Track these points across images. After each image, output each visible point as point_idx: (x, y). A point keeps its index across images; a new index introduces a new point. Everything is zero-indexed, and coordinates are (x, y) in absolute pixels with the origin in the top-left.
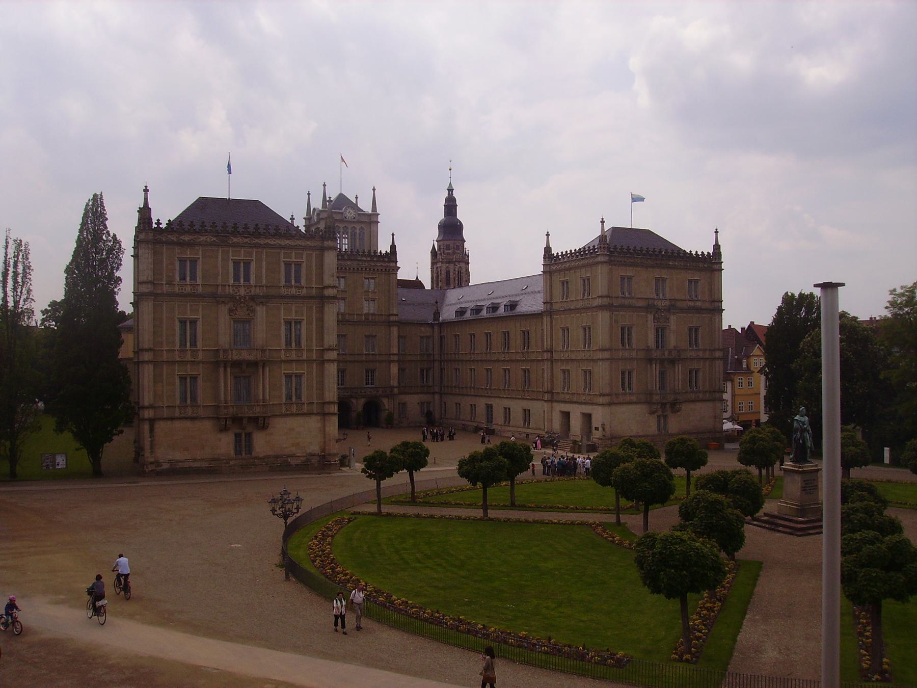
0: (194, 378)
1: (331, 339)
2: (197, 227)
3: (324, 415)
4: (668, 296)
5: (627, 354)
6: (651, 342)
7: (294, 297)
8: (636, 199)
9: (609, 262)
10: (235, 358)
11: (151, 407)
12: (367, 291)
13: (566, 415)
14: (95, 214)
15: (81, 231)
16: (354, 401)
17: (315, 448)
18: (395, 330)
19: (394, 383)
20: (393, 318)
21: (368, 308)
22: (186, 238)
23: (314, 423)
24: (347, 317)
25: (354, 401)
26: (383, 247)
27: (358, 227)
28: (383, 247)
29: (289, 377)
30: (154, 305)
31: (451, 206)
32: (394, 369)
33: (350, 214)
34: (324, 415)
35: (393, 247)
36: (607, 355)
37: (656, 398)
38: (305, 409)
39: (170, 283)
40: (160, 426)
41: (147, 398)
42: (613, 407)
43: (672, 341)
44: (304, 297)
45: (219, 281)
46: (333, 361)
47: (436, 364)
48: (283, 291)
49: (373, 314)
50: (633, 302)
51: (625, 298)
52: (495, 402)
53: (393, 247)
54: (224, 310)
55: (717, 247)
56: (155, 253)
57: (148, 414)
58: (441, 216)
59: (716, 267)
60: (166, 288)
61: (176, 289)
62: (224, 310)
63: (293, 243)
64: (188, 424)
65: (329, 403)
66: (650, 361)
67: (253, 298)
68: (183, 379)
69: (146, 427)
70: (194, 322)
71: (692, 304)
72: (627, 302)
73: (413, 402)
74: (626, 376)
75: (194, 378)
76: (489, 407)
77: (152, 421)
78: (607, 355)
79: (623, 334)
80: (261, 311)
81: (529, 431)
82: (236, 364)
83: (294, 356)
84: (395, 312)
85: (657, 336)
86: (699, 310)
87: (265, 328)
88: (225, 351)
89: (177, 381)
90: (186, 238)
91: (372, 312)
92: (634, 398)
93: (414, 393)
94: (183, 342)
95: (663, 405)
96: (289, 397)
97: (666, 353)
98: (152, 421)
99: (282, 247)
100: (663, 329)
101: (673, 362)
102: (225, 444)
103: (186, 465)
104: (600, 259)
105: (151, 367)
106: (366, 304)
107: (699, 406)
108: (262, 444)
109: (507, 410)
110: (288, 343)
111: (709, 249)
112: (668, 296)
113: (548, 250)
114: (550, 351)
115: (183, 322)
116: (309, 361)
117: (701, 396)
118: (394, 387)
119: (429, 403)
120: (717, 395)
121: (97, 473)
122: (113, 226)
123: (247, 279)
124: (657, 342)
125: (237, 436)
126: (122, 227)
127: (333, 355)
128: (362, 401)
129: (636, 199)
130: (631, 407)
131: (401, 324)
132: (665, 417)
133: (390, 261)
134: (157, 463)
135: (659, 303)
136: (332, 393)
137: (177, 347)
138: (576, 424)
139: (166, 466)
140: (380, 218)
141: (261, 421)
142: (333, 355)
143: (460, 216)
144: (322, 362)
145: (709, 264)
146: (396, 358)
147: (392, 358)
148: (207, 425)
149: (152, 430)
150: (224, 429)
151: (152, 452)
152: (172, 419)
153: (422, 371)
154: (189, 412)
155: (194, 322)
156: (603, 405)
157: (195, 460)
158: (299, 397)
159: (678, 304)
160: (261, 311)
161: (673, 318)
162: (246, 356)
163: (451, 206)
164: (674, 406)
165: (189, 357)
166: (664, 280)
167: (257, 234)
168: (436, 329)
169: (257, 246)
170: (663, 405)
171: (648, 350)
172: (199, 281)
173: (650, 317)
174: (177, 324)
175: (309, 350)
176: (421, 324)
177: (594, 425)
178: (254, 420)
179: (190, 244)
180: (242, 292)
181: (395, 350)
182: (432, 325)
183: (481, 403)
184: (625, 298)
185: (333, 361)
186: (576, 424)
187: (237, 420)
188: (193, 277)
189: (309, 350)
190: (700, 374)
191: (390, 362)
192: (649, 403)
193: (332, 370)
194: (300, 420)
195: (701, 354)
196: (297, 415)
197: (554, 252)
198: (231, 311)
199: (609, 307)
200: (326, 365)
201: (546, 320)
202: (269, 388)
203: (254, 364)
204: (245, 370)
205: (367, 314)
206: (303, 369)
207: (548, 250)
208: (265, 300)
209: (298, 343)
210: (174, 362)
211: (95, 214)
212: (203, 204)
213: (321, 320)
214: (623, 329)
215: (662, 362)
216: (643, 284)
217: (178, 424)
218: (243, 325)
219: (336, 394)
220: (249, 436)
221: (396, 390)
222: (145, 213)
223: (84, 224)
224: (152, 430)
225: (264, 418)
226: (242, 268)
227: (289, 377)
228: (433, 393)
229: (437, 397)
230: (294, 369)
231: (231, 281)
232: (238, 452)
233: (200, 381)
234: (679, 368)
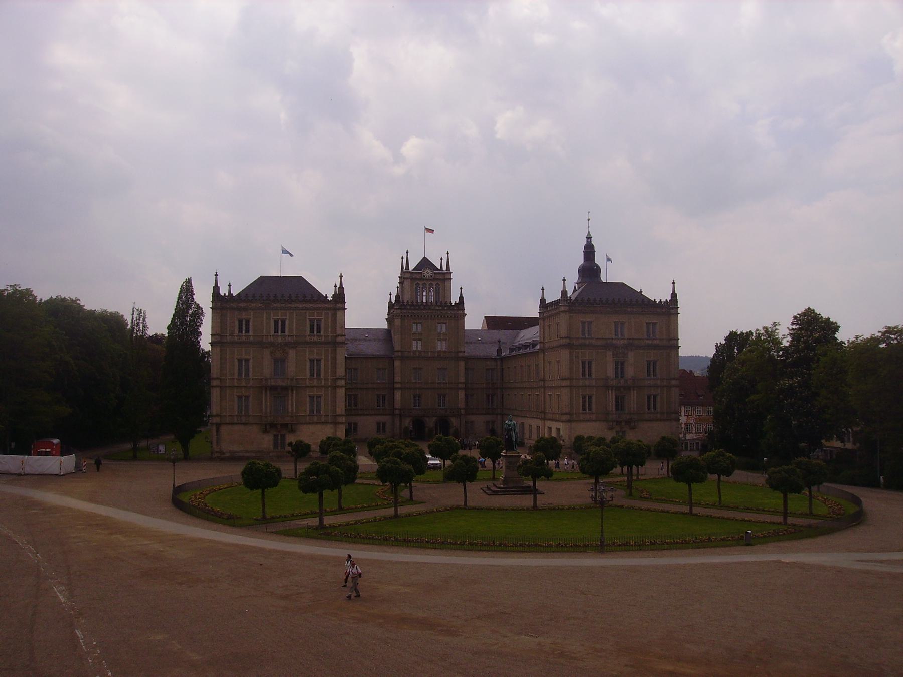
0: (247, 397)
1: (341, 371)
2: (251, 298)
3: (336, 423)
4: (626, 336)
5: (587, 382)
6: (610, 372)
7: (315, 343)
9: (570, 311)
10: (273, 384)
11: (217, 415)
12: (440, 334)
13: (550, 428)
14: (187, 291)
15: (178, 303)
16: (427, 419)
18: (462, 364)
19: (462, 405)
20: (461, 354)
21: (441, 346)
22: (243, 305)
24: (423, 354)
25: (427, 419)
26: (454, 300)
27: (434, 283)
28: (454, 300)
29: (311, 397)
30: (221, 350)
32: (462, 394)
33: (428, 273)
34: (336, 423)
35: (461, 298)
36: (567, 383)
39: (232, 335)
40: (224, 429)
41: (215, 409)
42: (574, 424)
43: (630, 372)
44: (321, 343)
45: (265, 333)
46: (342, 386)
48: (308, 339)
49: (445, 352)
50: (594, 341)
51: (585, 339)
53: (461, 298)
54: (267, 352)
55: (674, 295)
57: (216, 420)
58: (581, 261)
59: (672, 311)
60: (229, 339)
62: (267, 352)
63: (315, 306)
64: (242, 427)
65: (339, 415)
68: (240, 397)
69: (214, 428)
70: (247, 361)
71: (650, 342)
72: (587, 342)
73: (479, 421)
75: (247, 397)
77: (218, 426)
78: (567, 383)
79: (584, 367)
80: (292, 353)
82: (273, 388)
83: (315, 383)
84: (462, 349)
85: (616, 368)
86: (656, 347)
87: (296, 365)
88: (266, 379)
89: (236, 399)
90: (243, 305)
92: (594, 417)
94: (240, 374)
96: (312, 411)
97: (622, 381)
98: (218, 426)
99: (307, 309)
100: (622, 364)
103: (241, 454)
104: (563, 309)
105: (218, 389)
106: (439, 343)
110: (312, 374)
111: (666, 297)
112: (626, 336)
114: (544, 380)
115: (240, 361)
116: (326, 387)
117: (659, 416)
119: (493, 422)
120: (674, 416)
121: (186, 458)
122: (197, 298)
123: (283, 331)
124: (616, 373)
125: (276, 436)
126: (203, 298)
127: (343, 382)
128: (435, 418)
131: (467, 359)
133: (458, 310)
134: (222, 453)
135: (614, 342)
137: (236, 377)
139: (228, 455)
140: (452, 276)
141: (290, 426)
142: (343, 382)
144: (335, 387)
145: (670, 308)
146: (463, 386)
147: (460, 385)
149: (218, 431)
150: (266, 431)
151: (217, 445)
152: (232, 424)
153: (488, 396)
154: (244, 420)
155: (247, 361)
156: (563, 421)
157: (247, 452)
158: (318, 411)
160: (292, 353)
162: (280, 383)
165: (244, 384)
166: (622, 324)
167: (290, 301)
168: (499, 362)
169: (290, 309)
170: (618, 423)
172: (251, 333)
173: (609, 353)
174: (236, 361)
176: (486, 358)
178: (285, 426)
179: (245, 309)
180: (280, 340)
181: (462, 380)
182: (495, 359)
184: (585, 339)
185: (342, 386)
187: (273, 425)
188: (247, 331)
190: (658, 399)
193: (341, 393)
194: (319, 427)
195: (659, 382)
196: (317, 423)
198: (272, 353)
199: (570, 346)
200: (337, 390)
201: (541, 355)
203: (286, 388)
204: (280, 392)
205: (439, 352)
206: (321, 393)
207: (543, 301)
208: (295, 345)
209: (319, 374)
211: (187, 291)
212: (263, 281)
213: (334, 359)
214: (584, 363)
216: (604, 326)
217: (236, 428)
218: (280, 363)
219: (344, 409)
221: (463, 412)
222: (216, 288)
223: (180, 298)
224: (218, 431)
225: (292, 425)
226: (280, 326)
227: (311, 397)
229: (499, 417)
230: (315, 392)
231: (273, 333)
233: (251, 399)
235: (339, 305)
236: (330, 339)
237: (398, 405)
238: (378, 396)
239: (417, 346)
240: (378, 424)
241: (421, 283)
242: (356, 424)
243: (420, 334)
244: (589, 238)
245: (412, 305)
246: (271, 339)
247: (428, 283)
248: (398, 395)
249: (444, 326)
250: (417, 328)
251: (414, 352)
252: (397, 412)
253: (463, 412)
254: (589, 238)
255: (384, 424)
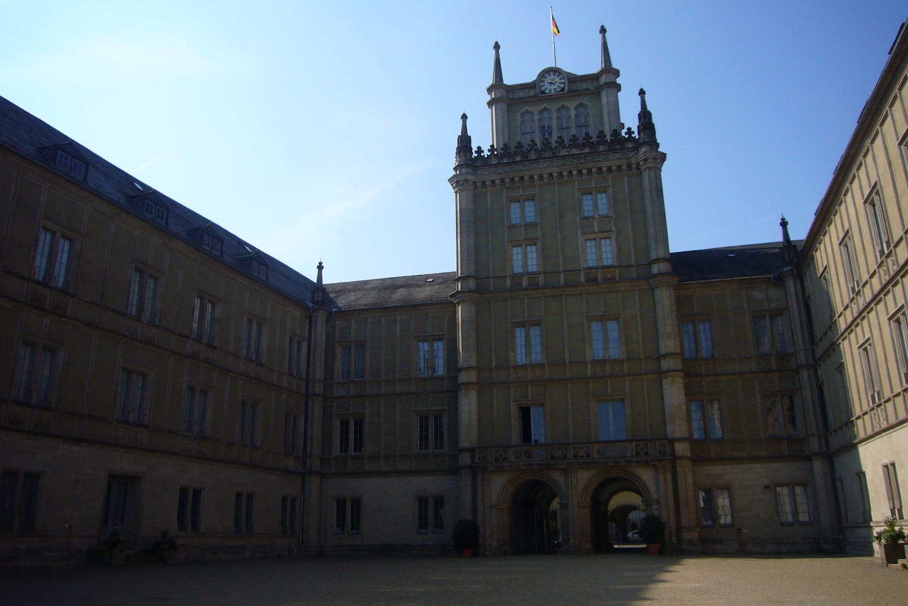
27: (572, 104)
35: (645, 117)
47: (804, 374)
53: (645, 117)
91: (606, 262)
93: (752, 459)
118: (672, 441)
147: (665, 364)
191: (662, 374)
228: (809, 459)
237: (468, 435)
238: (424, 420)
239: (525, 260)
240: (423, 501)
241: (535, 109)
242: (357, 503)
243: (529, 226)
245: (500, 157)
247: (553, 107)
248: (468, 406)
249: (602, 199)
250: (523, 213)
251: (516, 277)
252: (465, 459)
253: (681, 449)
255: (439, 501)
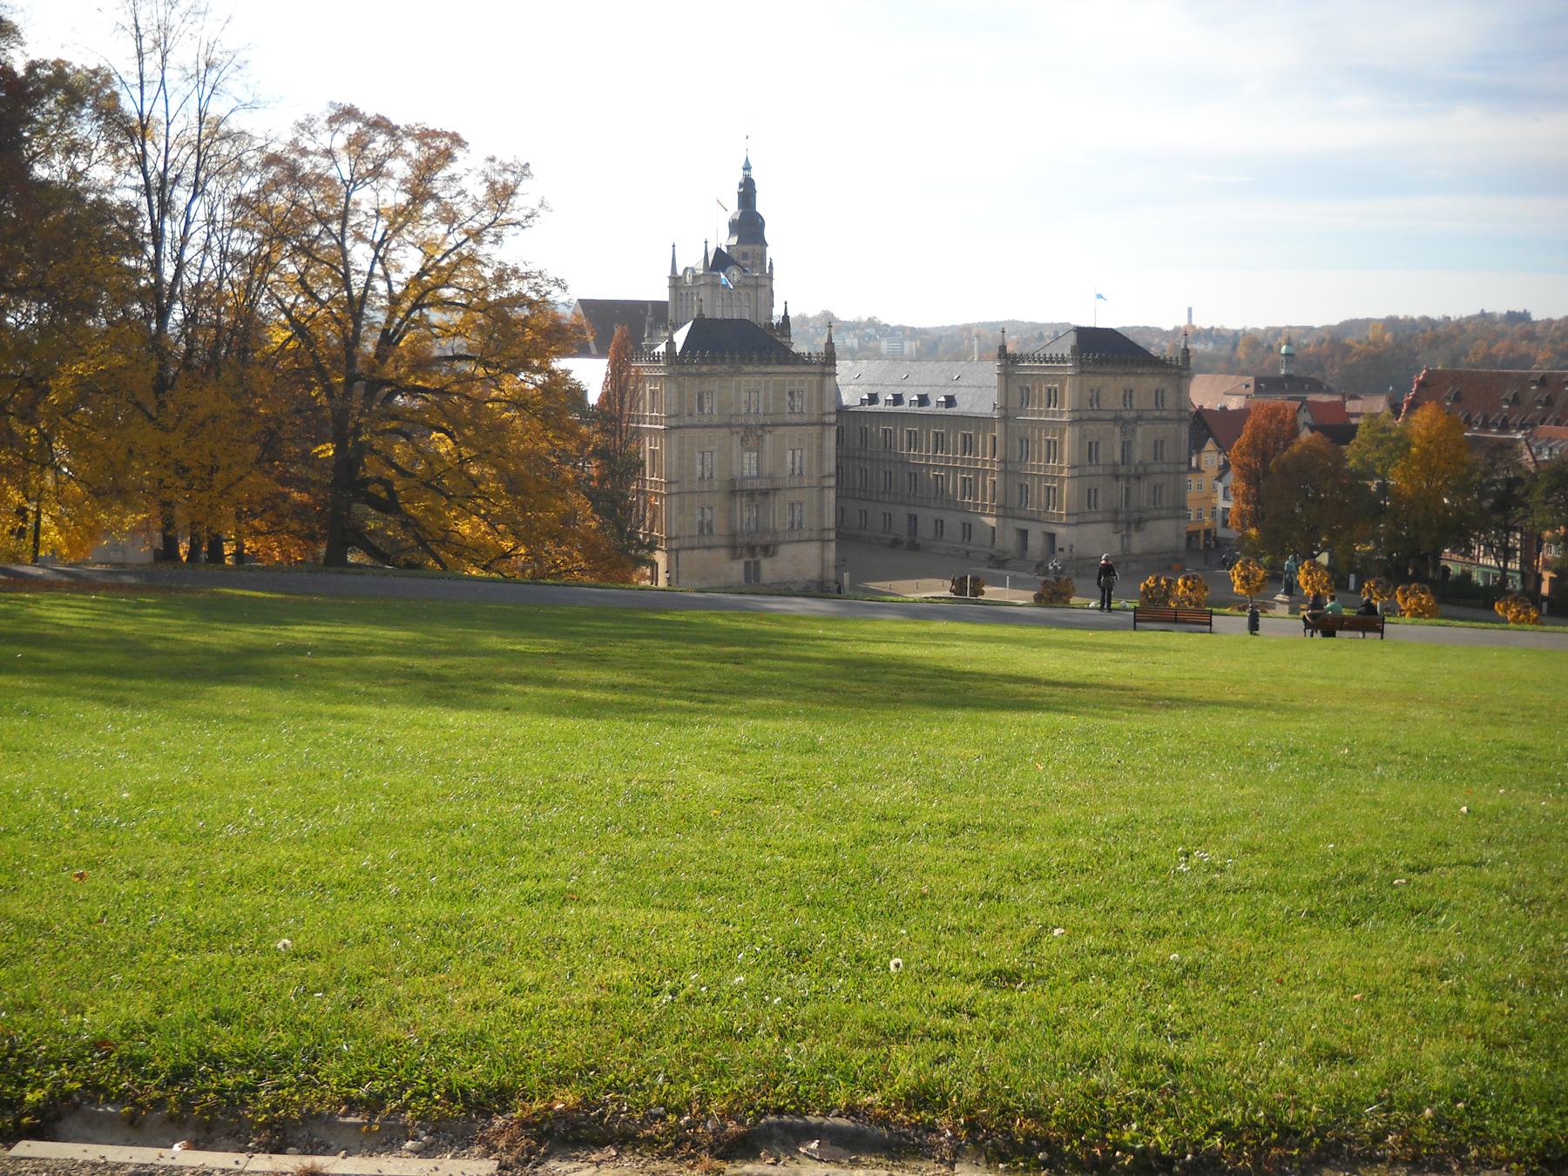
3: (823, 541)
5: (1093, 470)
6: (1118, 458)
8: (1099, 296)
13: (1024, 534)
17: (814, 574)
23: (813, 549)
31: (747, 192)
37: (1122, 517)
38: (806, 535)
43: (1138, 455)
48: (789, 419)
50: (1100, 415)
52: (922, 514)
56: (679, 386)
58: (733, 208)
61: (696, 421)
64: (705, 553)
66: (1117, 477)
67: (763, 426)
74: (1092, 495)
76: (913, 519)
81: (968, 548)
82: (751, 494)
92: (1099, 517)
95: (1129, 524)
100: (1129, 443)
101: (1138, 478)
102: (736, 570)
107: (1161, 524)
108: (769, 569)
109: (939, 524)
113: (1003, 348)
125: (747, 564)
129: (1099, 296)
130: (1096, 526)
132: (1129, 536)
133: (783, 335)
135: (1125, 414)
136: (830, 521)
138: (1036, 542)
143: (760, 208)
148: (722, 554)
152: (693, 548)
154: (707, 542)
159: (1146, 414)
161: (1139, 430)
163: (747, 192)
164: (1139, 524)
171: (1115, 465)
173: (1118, 430)
175: (810, 476)
177: (1058, 546)
183: (900, 514)
186: (1036, 542)
187: (752, 549)
189: (810, 476)
192: (1115, 522)
194: (801, 546)
195: (1165, 468)
197: (1010, 349)
202: (778, 516)
210: (692, 492)
215: (1128, 477)
217: (697, 553)
220: (757, 563)
232: (747, 580)
234: (1145, 485)
235: (827, 370)
236: (814, 418)
244: (747, 167)
246: (742, 420)
254: (747, 167)
